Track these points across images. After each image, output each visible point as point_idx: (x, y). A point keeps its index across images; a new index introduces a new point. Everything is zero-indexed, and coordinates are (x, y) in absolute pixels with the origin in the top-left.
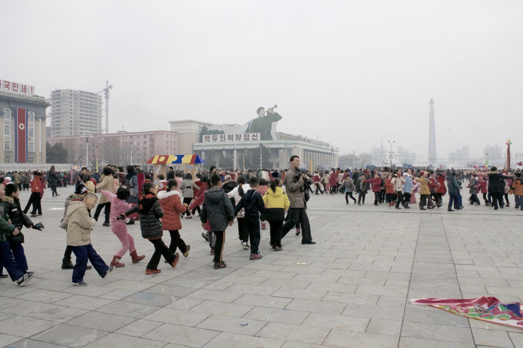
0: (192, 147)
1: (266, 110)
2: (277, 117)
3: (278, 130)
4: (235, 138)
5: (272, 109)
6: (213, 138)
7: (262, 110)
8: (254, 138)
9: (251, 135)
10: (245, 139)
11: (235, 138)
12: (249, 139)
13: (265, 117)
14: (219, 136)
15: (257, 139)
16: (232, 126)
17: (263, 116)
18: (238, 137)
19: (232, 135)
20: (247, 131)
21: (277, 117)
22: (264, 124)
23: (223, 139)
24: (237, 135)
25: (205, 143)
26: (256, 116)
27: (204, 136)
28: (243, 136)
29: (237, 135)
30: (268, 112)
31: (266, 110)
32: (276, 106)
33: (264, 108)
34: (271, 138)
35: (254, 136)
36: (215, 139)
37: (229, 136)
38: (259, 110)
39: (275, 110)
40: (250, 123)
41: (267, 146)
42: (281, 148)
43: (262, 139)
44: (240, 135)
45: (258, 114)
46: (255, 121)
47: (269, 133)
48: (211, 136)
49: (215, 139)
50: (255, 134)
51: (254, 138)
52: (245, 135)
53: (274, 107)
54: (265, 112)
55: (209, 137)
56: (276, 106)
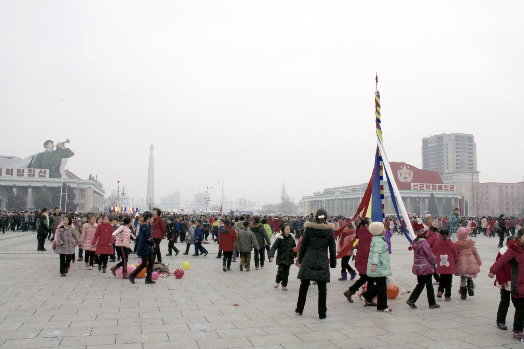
1: (55, 144)
2: (68, 154)
3: (66, 169)
4: (15, 173)
5: (64, 144)
7: (50, 143)
8: (41, 174)
9: (38, 171)
10: (29, 175)
11: (15, 173)
12: (34, 175)
13: (53, 151)
15: (45, 176)
16: (9, 158)
17: (51, 151)
18: (20, 173)
19: (12, 170)
20: (30, 166)
21: (68, 154)
22: (52, 158)
24: (19, 170)
26: (43, 150)
28: (26, 171)
29: (19, 170)
30: (57, 146)
31: (55, 144)
32: (68, 141)
33: (52, 142)
34: (59, 176)
35: (41, 172)
38: (46, 144)
39: (67, 146)
40: (33, 157)
41: (72, 185)
43: (51, 176)
44: (23, 171)
45: (45, 147)
46: (41, 155)
47: (57, 169)
50: (43, 170)
51: (41, 174)
52: (30, 171)
53: (65, 142)
54: (53, 146)
56: (68, 141)
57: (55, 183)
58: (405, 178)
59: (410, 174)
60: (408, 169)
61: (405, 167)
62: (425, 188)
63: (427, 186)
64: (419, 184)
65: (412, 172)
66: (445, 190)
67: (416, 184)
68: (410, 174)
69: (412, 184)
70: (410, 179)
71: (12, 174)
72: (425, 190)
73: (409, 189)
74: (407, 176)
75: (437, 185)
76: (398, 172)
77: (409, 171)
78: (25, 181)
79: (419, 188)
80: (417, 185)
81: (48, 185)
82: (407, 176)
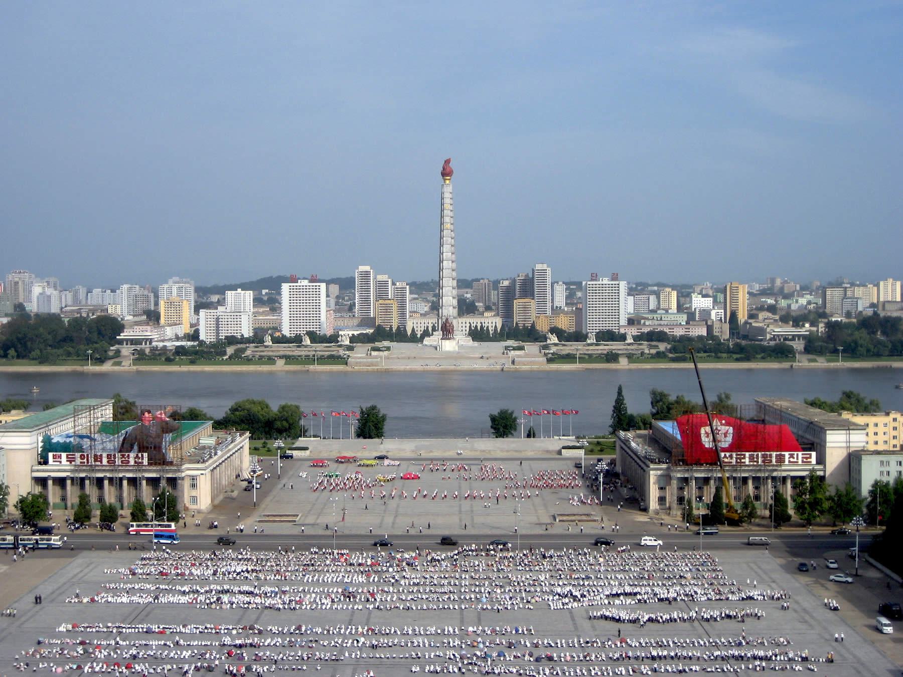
0: (32, 471)
6: (67, 457)
14: (78, 455)
19: (101, 456)
23: (85, 460)
27: (51, 455)
29: (109, 456)
35: (137, 457)
37: (96, 456)
42: (183, 479)
43: (152, 461)
44: (115, 455)
48: (64, 455)
49: (71, 460)
52: (123, 456)
55: (60, 457)
59: (725, 435)
60: (722, 424)
62: (747, 461)
63: (751, 458)
64: (734, 455)
65: (731, 430)
66: (790, 462)
67: (728, 454)
68: (725, 436)
71: (101, 462)
72: (747, 463)
75: (774, 454)
76: (703, 431)
79: (734, 461)
80: (731, 457)
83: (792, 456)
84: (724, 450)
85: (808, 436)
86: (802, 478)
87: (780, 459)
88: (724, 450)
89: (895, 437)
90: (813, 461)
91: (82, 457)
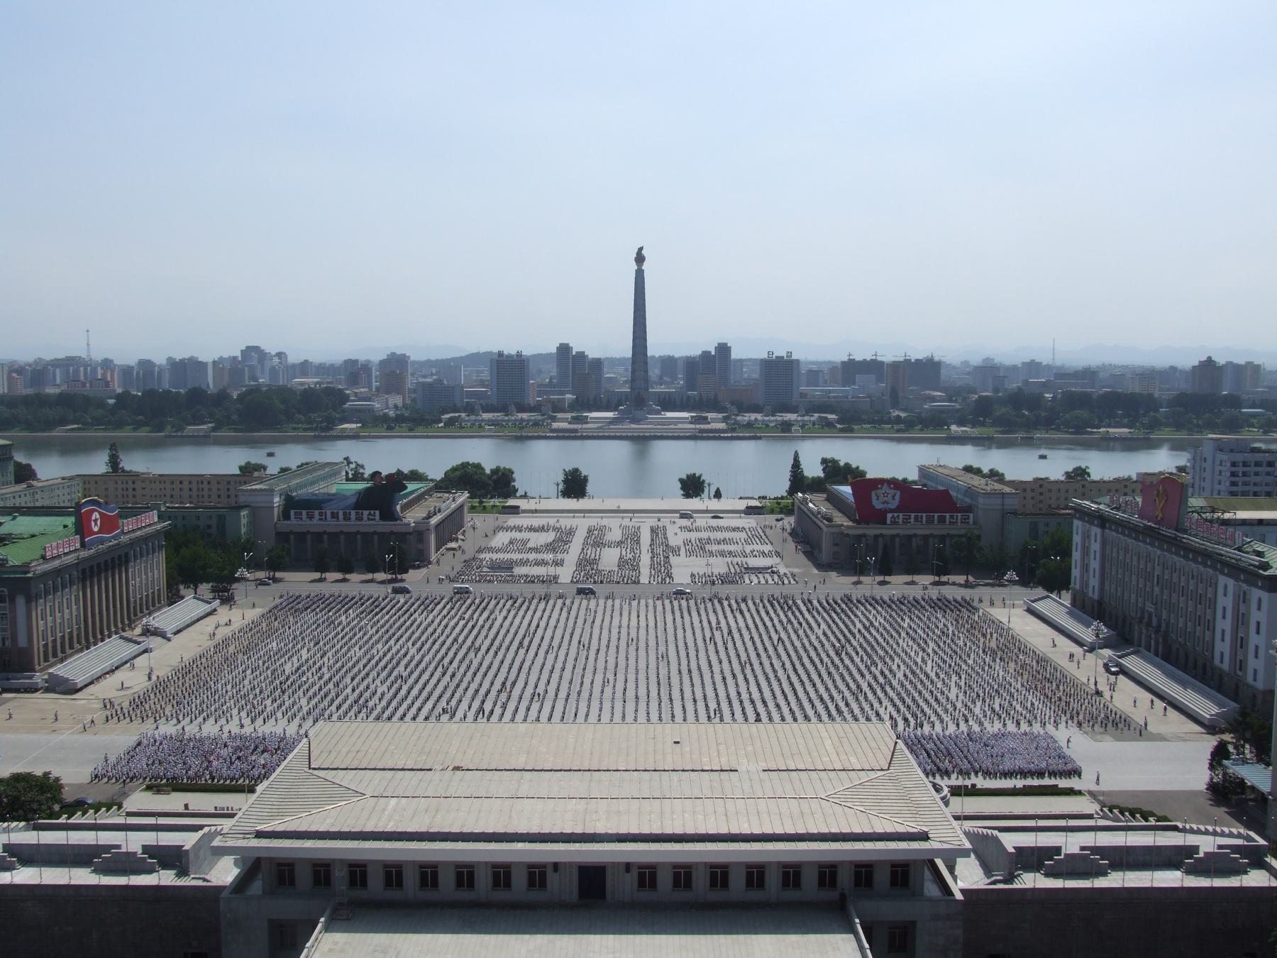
9: (366, 513)
12: (362, 519)
14: (316, 512)
25: (293, 521)
27: (292, 512)
28: (353, 512)
29: (345, 514)
36: (311, 517)
43: (383, 518)
48: (304, 512)
57: (386, 527)
58: (885, 502)
59: (893, 497)
61: (885, 486)
63: (916, 518)
65: (898, 493)
68: (893, 497)
69: (889, 516)
70: (894, 504)
73: (885, 523)
74: (889, 498)
76: (873, 493)
77: (892, 492)
78: (353, 525)
81: (379, 530)
82: (889, 498)
83: (952, 517)
84: (892, 511)
85: (967, 500)
86: (960, 536)
87: (942, 520)
88: (892, 511)
89: (1041, 502)
90: (971, 520)
91: (321, 514)
